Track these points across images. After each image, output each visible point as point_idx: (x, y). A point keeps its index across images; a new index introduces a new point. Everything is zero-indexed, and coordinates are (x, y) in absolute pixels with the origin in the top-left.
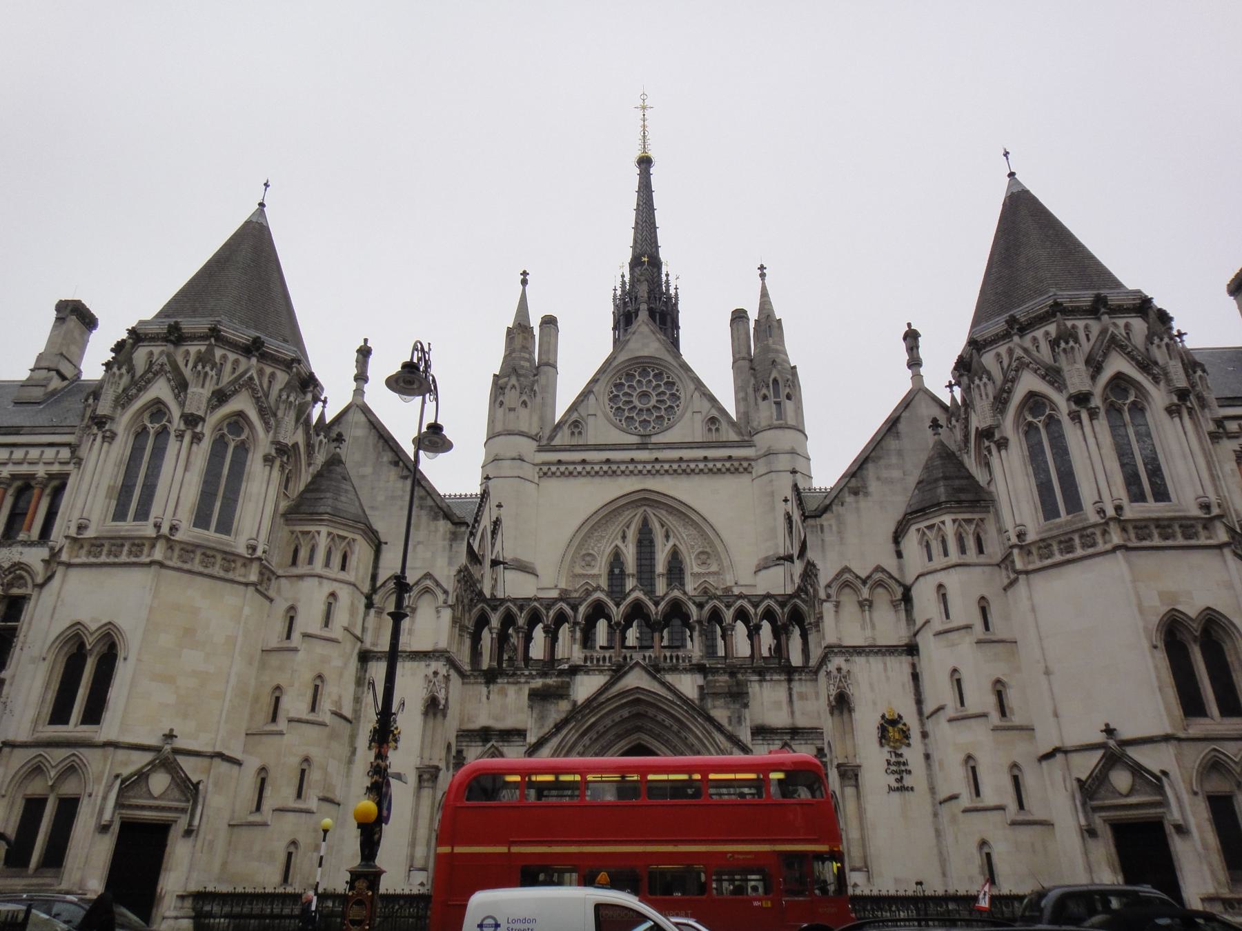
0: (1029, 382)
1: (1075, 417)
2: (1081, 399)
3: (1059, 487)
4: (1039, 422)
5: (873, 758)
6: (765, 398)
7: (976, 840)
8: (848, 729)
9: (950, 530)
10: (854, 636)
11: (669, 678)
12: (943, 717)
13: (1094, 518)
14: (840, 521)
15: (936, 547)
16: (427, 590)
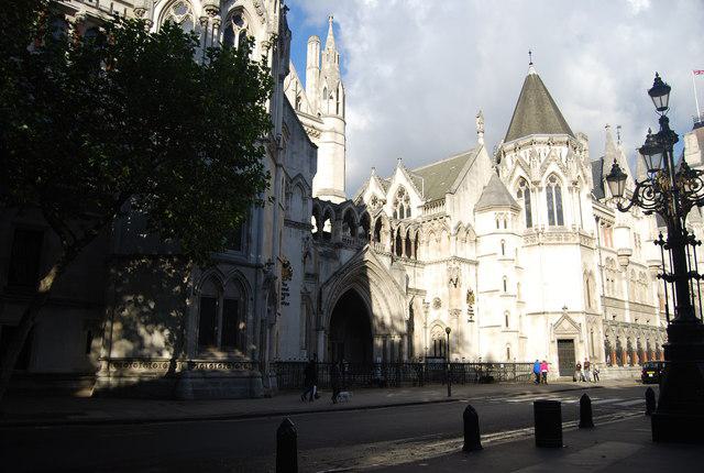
0: (553, 167)
1: (570, 189)
2: (575, 183)
3: (556, 215)
4: (553, 185)
5: (465, 307)
6: (331, 98)
7: (506, 342)
8: (458, 295)
9: (510, 216)
10: (461, 255)
11: (380, 257)
12: (497, 295)
13: (570, 230)
14: (459, 201)
15: (502, 224)
16: (299, 185)
